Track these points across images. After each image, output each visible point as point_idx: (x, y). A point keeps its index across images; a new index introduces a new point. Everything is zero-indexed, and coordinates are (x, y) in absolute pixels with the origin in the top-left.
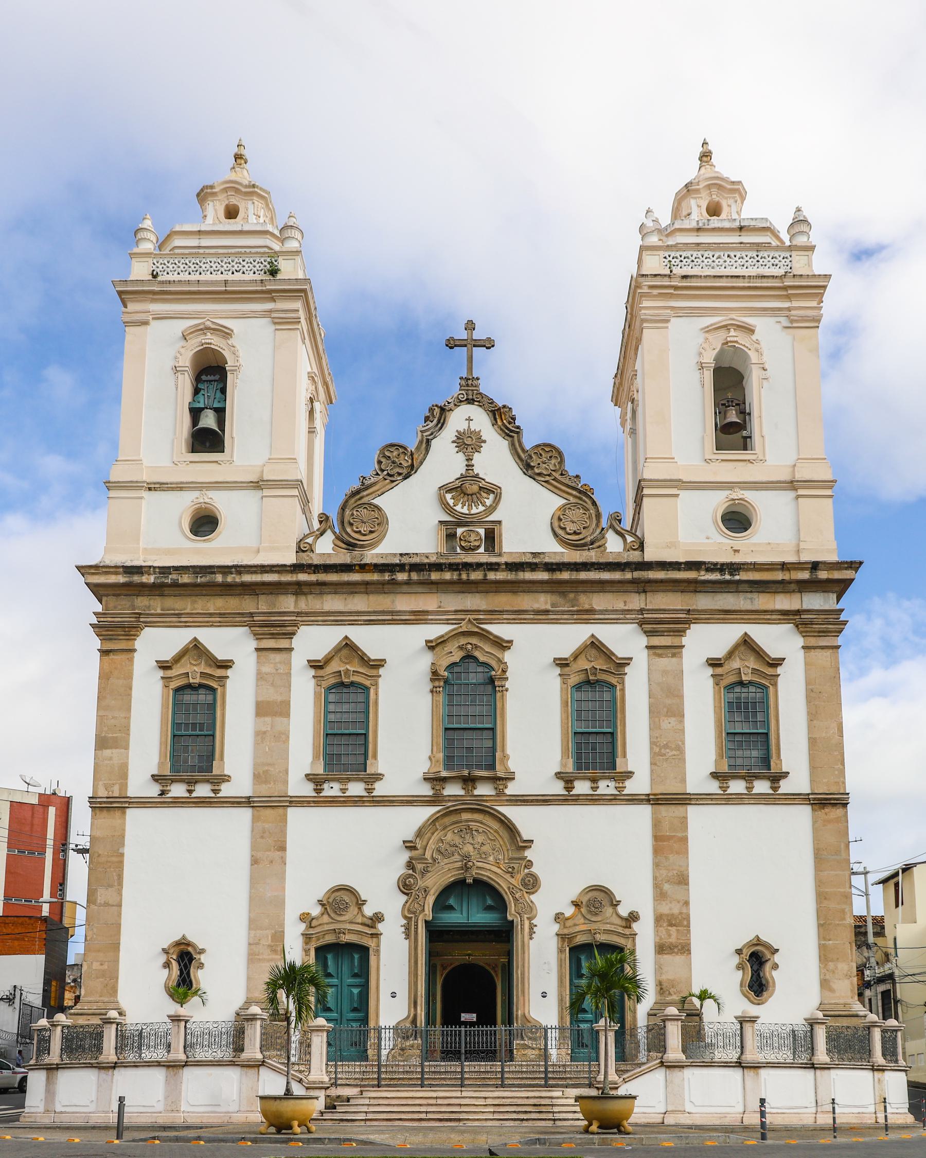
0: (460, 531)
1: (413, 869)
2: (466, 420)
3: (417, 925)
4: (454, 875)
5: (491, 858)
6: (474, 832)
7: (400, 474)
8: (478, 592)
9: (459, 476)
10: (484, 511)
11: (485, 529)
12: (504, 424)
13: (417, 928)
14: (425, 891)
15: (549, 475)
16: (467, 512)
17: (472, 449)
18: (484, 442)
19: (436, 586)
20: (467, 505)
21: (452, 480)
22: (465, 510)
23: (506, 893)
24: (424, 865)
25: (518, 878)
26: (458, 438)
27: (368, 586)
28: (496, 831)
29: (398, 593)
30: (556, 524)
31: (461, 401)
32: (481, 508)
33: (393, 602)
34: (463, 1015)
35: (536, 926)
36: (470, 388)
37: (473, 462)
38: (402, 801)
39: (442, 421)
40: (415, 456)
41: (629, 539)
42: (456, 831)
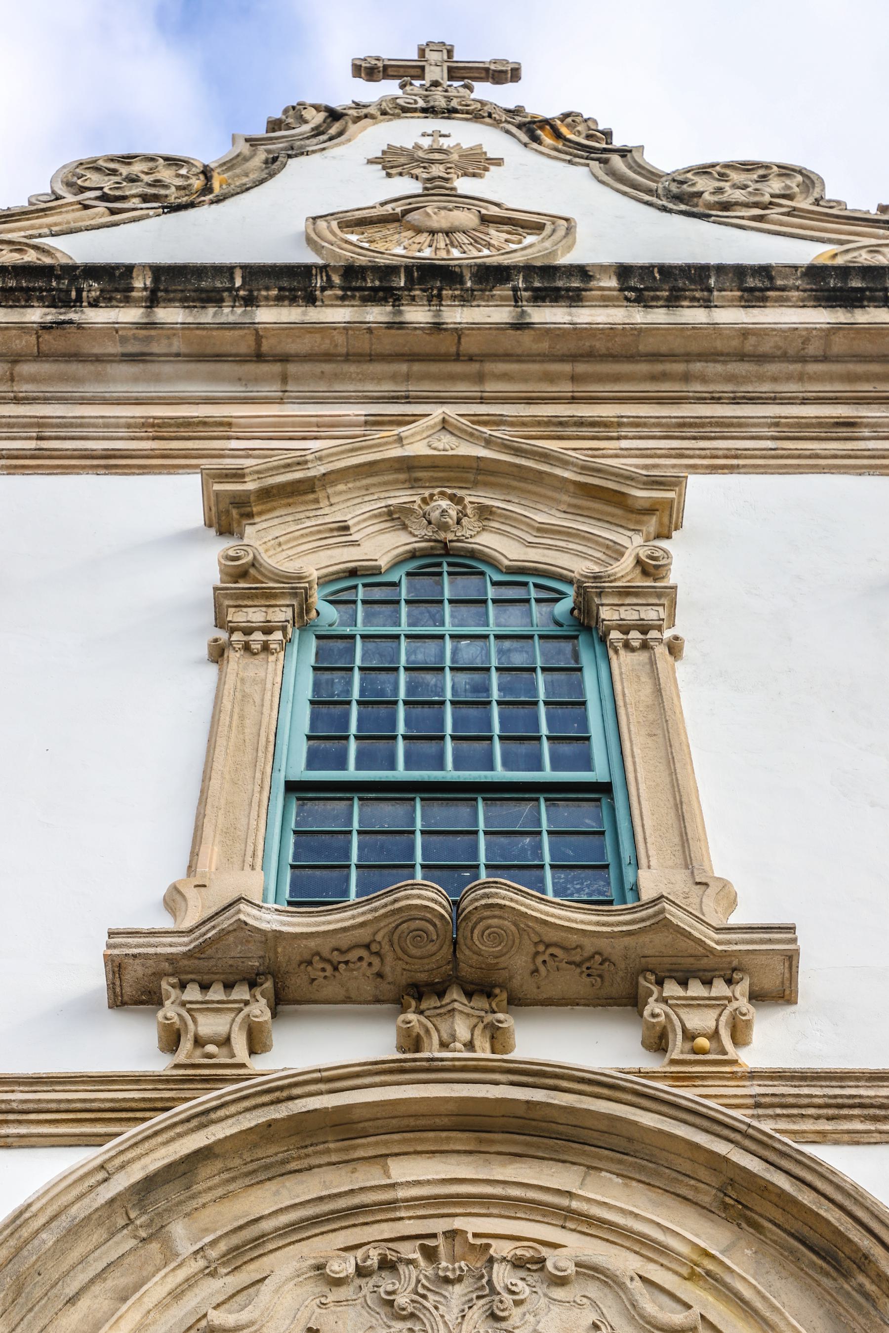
6: (502, 1275)
19: (277, 368)
42: (344, 1266)
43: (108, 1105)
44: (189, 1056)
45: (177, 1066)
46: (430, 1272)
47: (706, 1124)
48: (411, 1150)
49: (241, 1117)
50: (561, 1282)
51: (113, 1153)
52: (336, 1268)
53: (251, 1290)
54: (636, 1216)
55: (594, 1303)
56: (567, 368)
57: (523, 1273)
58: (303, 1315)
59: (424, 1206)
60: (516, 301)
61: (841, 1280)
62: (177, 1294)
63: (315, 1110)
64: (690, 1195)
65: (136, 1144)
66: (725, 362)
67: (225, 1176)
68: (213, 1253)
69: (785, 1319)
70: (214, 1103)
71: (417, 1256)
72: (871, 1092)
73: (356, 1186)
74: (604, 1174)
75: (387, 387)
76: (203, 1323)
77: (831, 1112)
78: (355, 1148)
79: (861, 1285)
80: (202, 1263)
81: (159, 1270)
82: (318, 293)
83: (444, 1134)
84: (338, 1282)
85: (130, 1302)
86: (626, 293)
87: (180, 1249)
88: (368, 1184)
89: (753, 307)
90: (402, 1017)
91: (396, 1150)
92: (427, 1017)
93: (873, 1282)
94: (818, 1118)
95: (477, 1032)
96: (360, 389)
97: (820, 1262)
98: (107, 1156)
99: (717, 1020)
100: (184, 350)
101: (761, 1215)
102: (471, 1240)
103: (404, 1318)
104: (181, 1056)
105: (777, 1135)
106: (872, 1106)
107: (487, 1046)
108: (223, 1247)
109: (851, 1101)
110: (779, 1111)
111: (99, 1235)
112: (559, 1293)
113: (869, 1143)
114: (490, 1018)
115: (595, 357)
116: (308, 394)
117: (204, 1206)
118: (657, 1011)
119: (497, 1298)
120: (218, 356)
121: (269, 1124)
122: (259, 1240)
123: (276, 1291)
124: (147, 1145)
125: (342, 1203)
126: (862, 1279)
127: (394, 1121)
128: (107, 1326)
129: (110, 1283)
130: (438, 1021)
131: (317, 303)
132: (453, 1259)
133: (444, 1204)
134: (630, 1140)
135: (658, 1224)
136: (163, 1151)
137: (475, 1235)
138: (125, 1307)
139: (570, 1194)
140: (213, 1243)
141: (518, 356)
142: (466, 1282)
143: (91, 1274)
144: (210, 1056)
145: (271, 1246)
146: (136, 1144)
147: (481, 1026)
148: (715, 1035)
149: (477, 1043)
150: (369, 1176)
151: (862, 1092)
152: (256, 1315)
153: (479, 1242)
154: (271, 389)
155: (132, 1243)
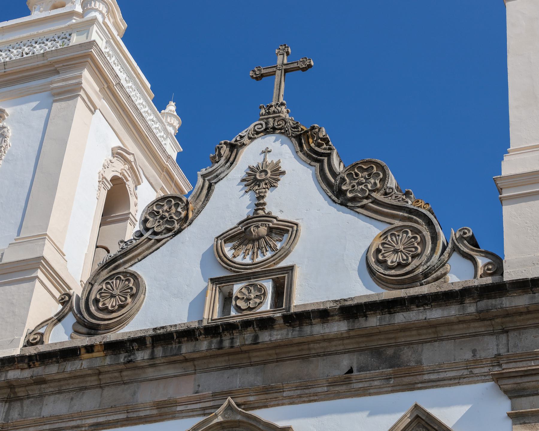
0: (237, 288)
2: (263, 152)
7: (169, 230)
8: (251, 365)
9: (245, 217)
10: (272, 257)
11: (273, 280)
12: (312, 150)
15: (367, 198)
16: (250, 262)
17: (266, 184)
18: (283, 173)
19: (191, 363)
20: (250, 253)
21: (235, 225)
22: (248, 260)
26: (249, 175)
27: (101, 377)
29: (141, 382)
30: (372, 260)
31: (258, 133)
32: (268, 254)
33: (135, 393)
36: (271, 116)
37: (265, 200)
39: (231, 159)
40: (191, 206)
41: (481, 261)
56: (273, 352)
60: (255, 331)
66: (319, 343)
75: (224, 364)
82: (198, 337)
86: (286, 324)
89: (325, 323)
96: (216, 366)
100: (165, 361)
115: (281, 346)
116: (202, 370)
120: (175, 361)
131: (199, 340)
141: (259, 349)
154: (191, 370)
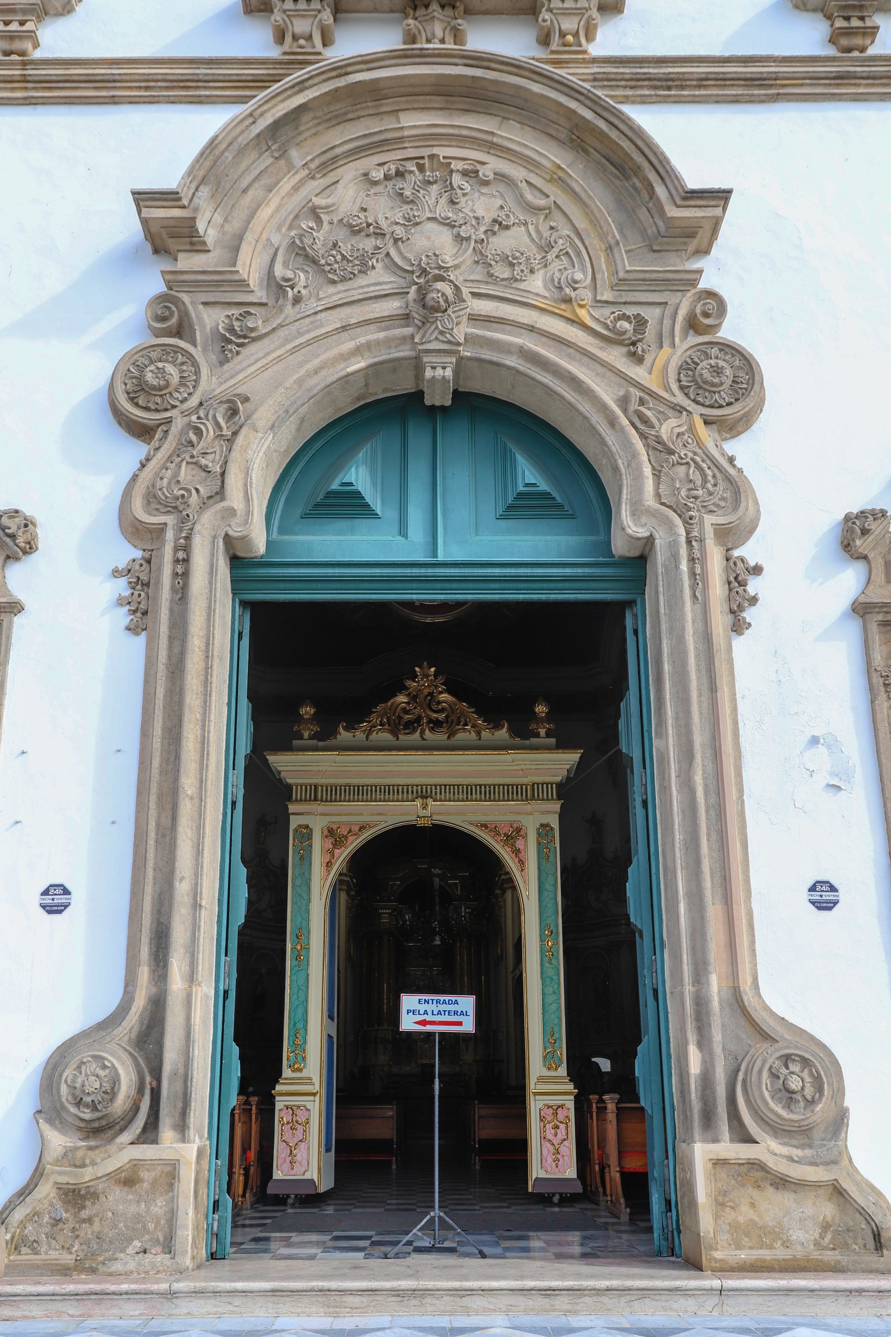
1: (182, 330)
3: (186, 561)
4: (368, 346)
5: (537, 283)
6: (457, 179)
13: (186, 575)
14: (233, 412)
23: (612, 422)
24: (235, 312)
25: (659, 363)
28: (558, 179)
34: (408, 1001)
35: (757, 570)
38: (148, 83)
43: (250, 78)
44: (291, 47)
45: (285, 53)
46: (421, 178)
47: (566, 90)
48: (411, 107)
49: (321, 85)
50: (486, 183)
51: (256, 106)
52: (374, 175)
53: (333, 187)
54: (526, 146)
55: (502, 196)
57: (467, 179)
58: (359, 200)
59: (418, 140)
61: (625, 181)
62: (296, 188)
63: (360, 82)
64: (554, 133)
65: (267, 101)
67: (315, 122)
68: (313, 166)
69: (595, 202)
70: (306, 76)
71: (414, 168)
72: (656, 71)
73: (383, 129)
74: (511, 122)
76: (310, 204)
77: (632, 83)
78: (381, 105)
79: (634, 184)
80: (307, 172)
81: (285, 175)
83: (428, 97)
84: (375, 183)
85: (273, 192)
87: (296, 164)
88: (389, 127)
90: (406, 22)
91: (403, 107)
92: (419, 22)
93: (640, 181)
94: (625, 87)
95: (447, 32)
97: (615, 171)
98: (253, 108)
99: (579, 24)
101: (589, 145)
102: (442, 160)
103: (408, 203)
104: (286, 47)
105: (603, 97)
106: (655, 79)
107: (452, 41)
108: (317, 162)
109: (644, 77)
110: (606, 83)
111: (254, 155)
112: (484, 190)
113: (650, 103)
114: (454, 22)
117: (305, 139)
118: (547, 17)
119: (454, 192)
121: (336, 90)
122: (334, 159)
123: (345, 188)
124: (273, 102)
125: (376, 138)
126: (635, 180)
127: (402, 89)
128: (263, 206)
129: (263, 182)
130: (425, 24)
132: (433, 171)
133: (428, 140)
134: (526, 101)
135: (537, 151)
136: (281, 106)
137: (444, 157)
138: (271, 195)
139: (492, 133)
140: (312, 160)
142: (440, 183)
143: (253, 177)
144: (302, 47)
145: (341, 163)
146: (267, 101)
147: (449, 28)
148: (576, 34)
149: (446, 39)
150: (389, 123)
151: (651, 71)
152: (336, 200)
153: (445, 161)
155: (271, 160)
